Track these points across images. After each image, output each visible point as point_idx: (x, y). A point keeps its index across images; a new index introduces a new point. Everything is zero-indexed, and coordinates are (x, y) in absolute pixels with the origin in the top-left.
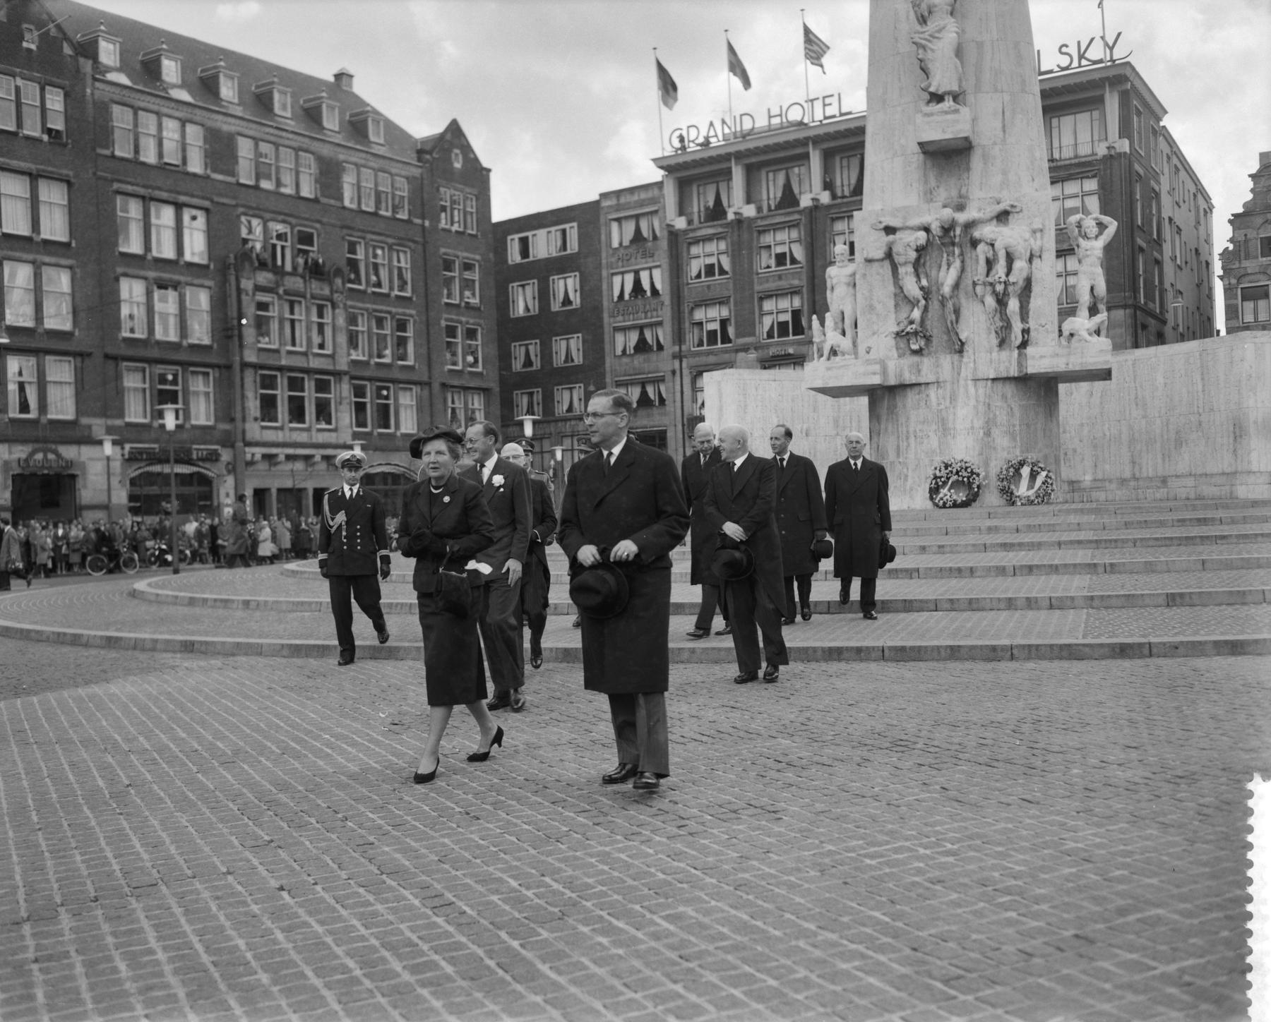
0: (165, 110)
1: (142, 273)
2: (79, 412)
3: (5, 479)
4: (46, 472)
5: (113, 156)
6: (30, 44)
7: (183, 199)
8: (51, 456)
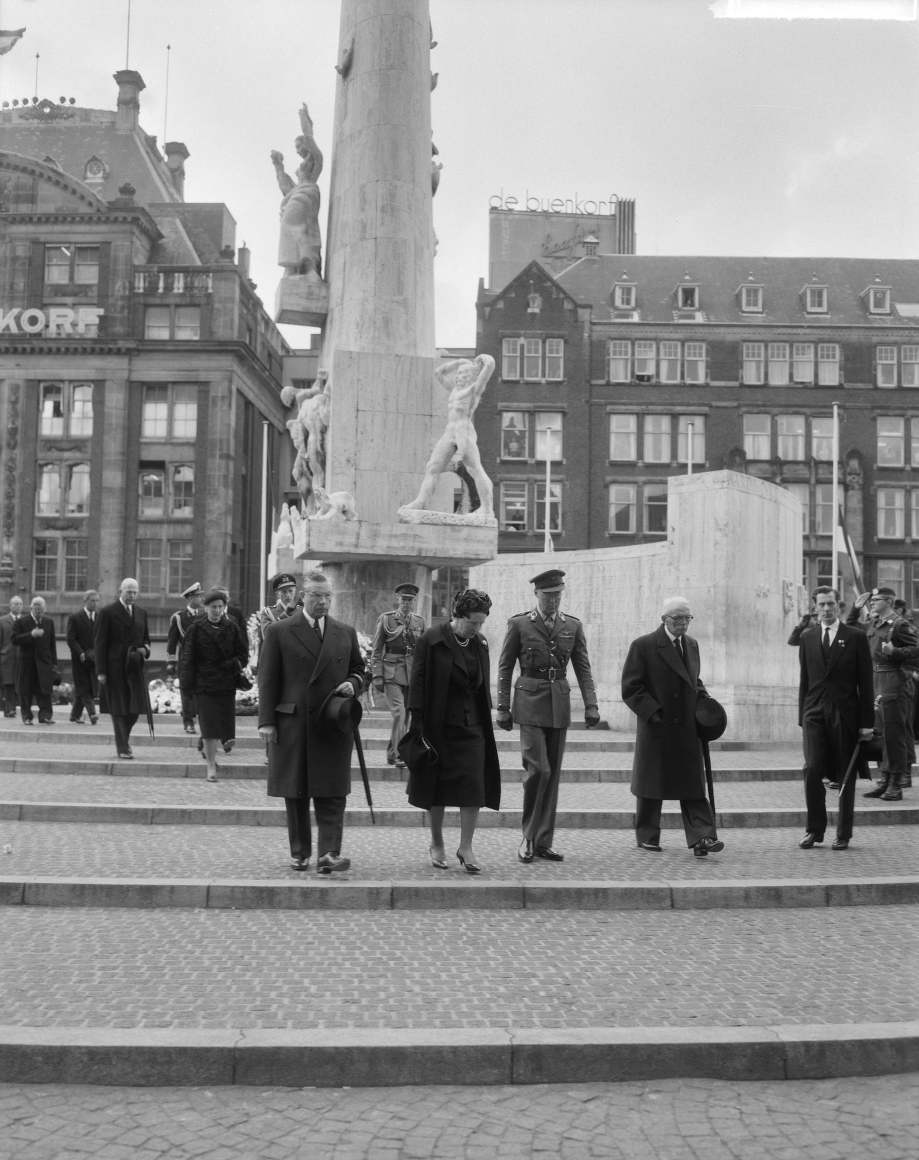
0: (660, 335)
5: (608, 384)
6: (535, 308)
7: (678, 409)
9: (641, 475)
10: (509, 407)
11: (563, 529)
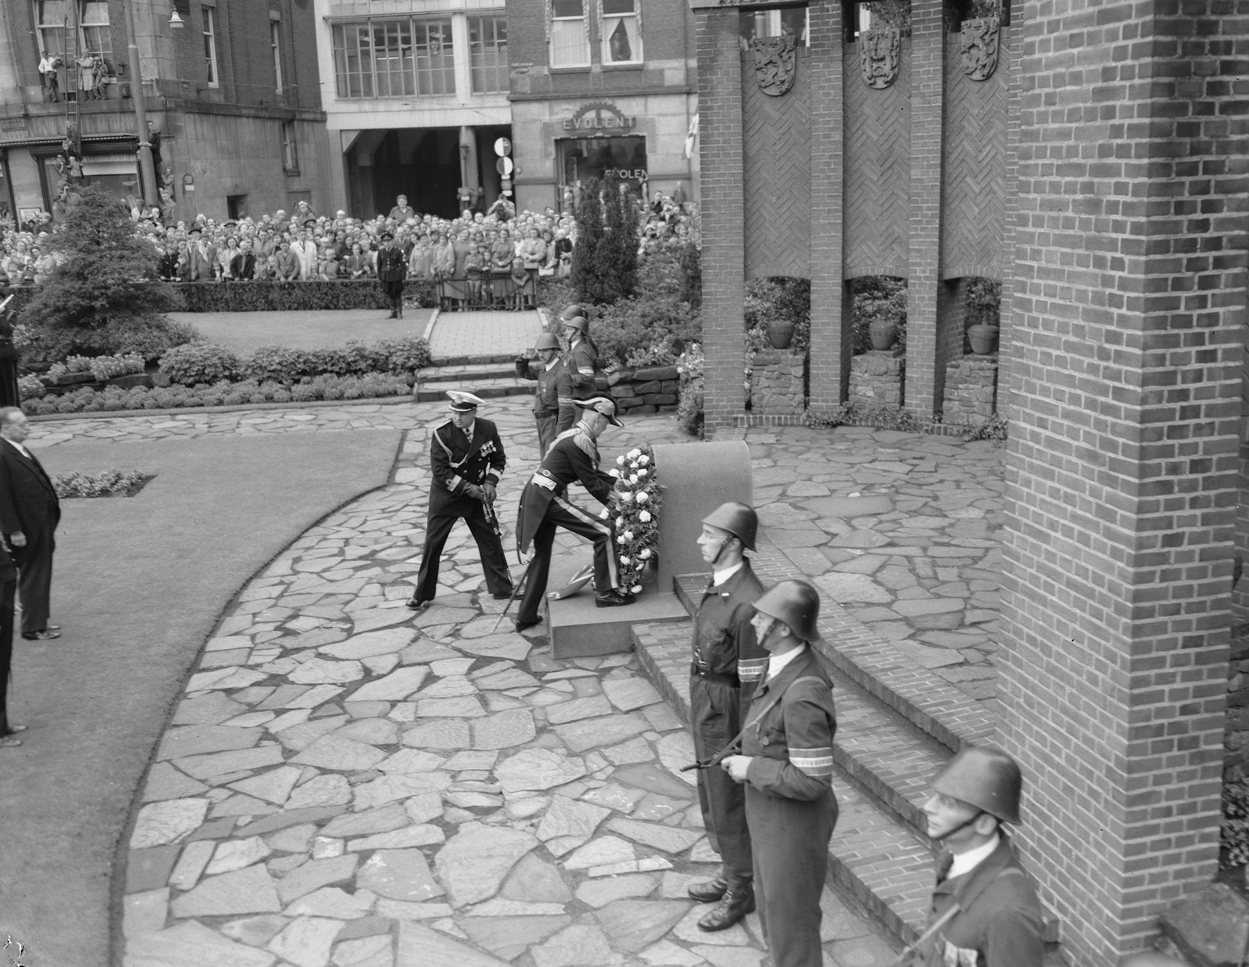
2: (648, 55)
4: (599, 134)
8: (606, 114)
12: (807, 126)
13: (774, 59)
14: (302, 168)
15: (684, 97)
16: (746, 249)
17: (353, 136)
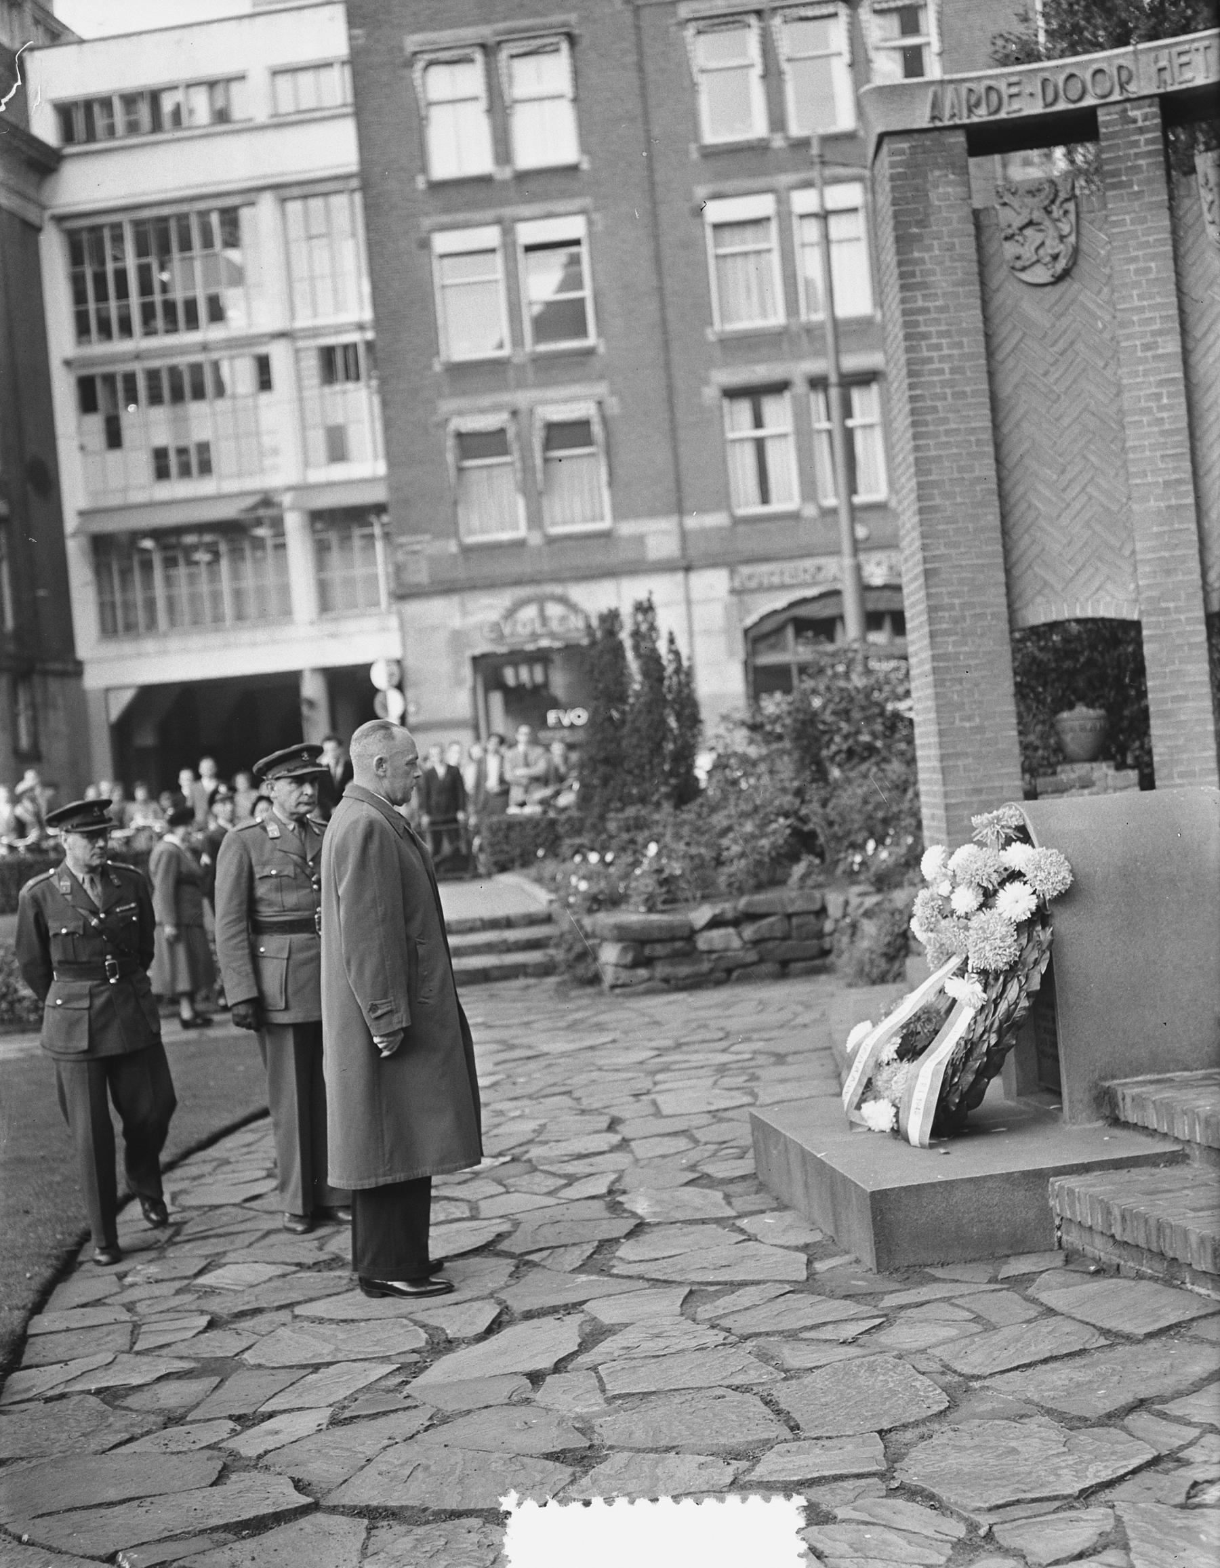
1: (761, 182)
2: (619, 513)
3: (458, 665)
4: (545, 643)
8: (554, 610)
9: (782, 170)
10: (434, 43)
11: (600, 334)
12: (1107, 336)
13: (1037, 215)
14: (44, 748)
15: (680, 576)
16: (1008, 571)
17: (127, 696)
